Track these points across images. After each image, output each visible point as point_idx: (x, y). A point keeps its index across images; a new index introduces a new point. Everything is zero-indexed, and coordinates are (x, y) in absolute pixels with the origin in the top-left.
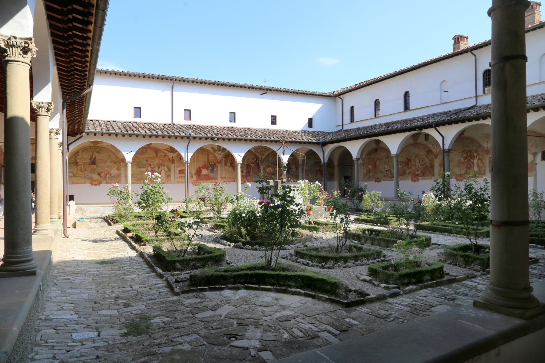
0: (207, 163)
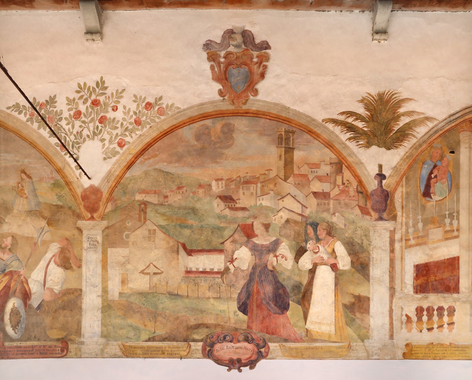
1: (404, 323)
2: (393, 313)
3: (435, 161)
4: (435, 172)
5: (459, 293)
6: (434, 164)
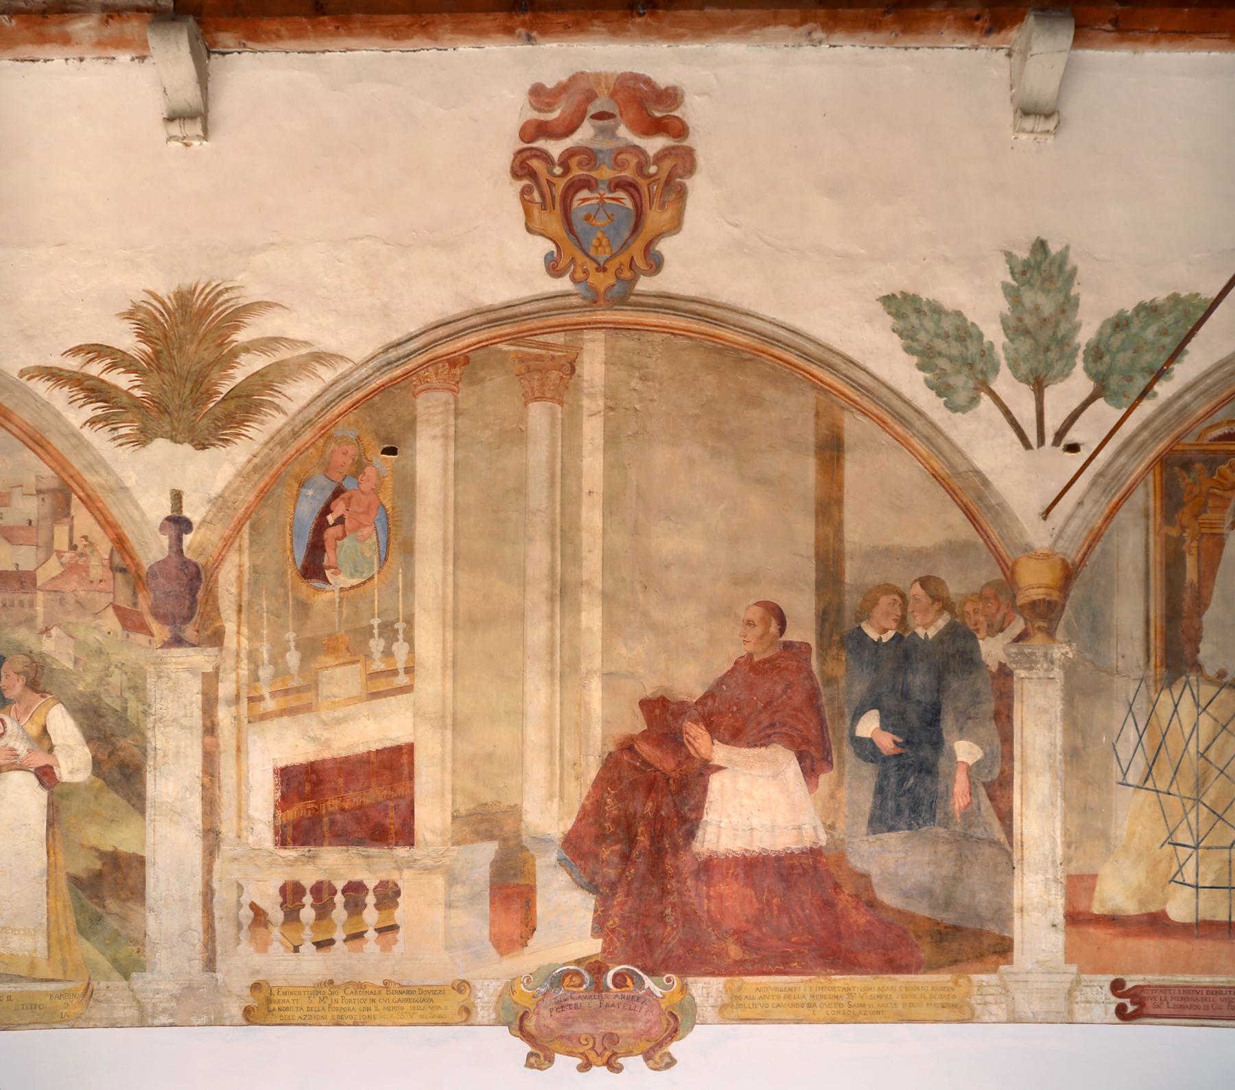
0: (803, 630)
1: (245, 927)
2: (214, 900)
3: (337, 477)
4: (339, 508)
5: (412, 845)
6: (334, 486)
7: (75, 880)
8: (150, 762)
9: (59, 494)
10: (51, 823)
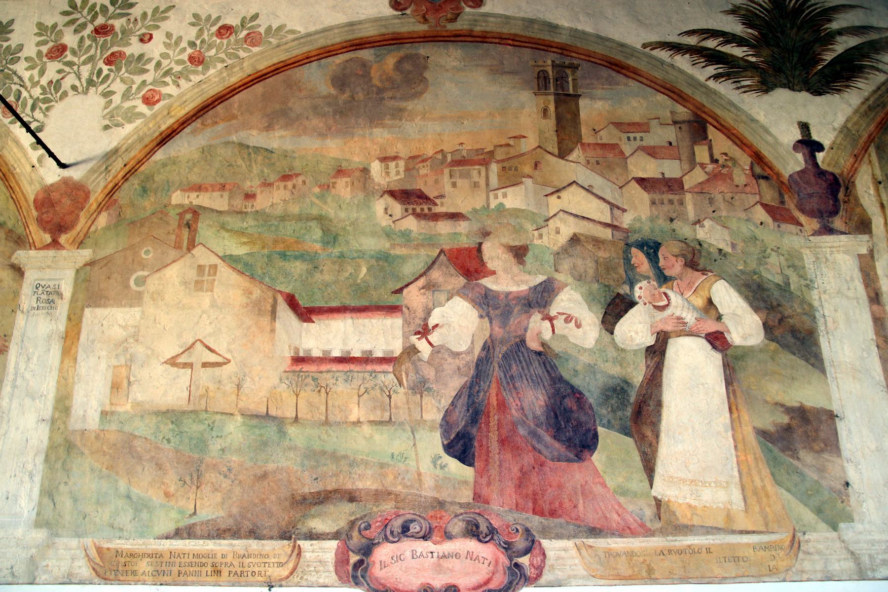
7: (763, 434)
8: (821, 328)
9: (695, 124)
10: (729, 382)
